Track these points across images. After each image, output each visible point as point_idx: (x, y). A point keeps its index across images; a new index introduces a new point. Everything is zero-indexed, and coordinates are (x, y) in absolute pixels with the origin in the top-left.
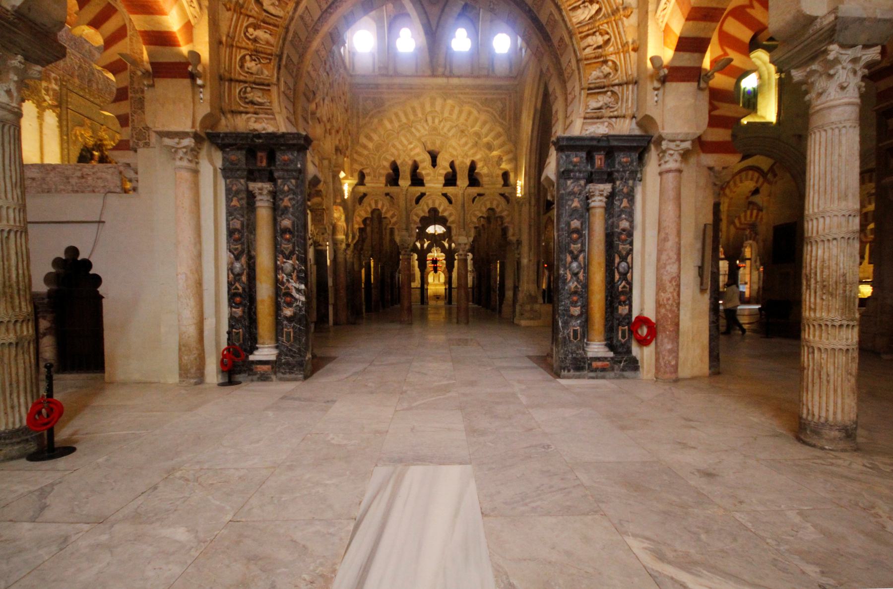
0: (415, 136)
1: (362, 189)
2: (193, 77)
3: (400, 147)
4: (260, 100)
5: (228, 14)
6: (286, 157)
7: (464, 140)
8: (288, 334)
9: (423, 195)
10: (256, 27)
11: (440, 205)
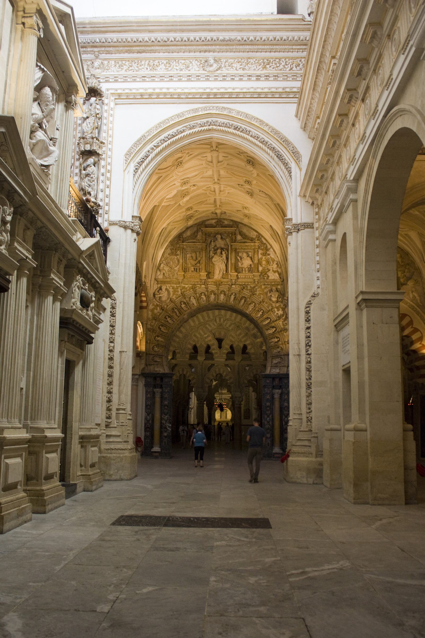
0: (209, 329)
1: (173, 362)
2: (140, 357)
3: (198, 336)
4: (158, 361)
5: (149, 332)
6: (166, 380)
7: (239, 332)
8: (165, 442)
9: (213, 365)
10: (158, 336)
11: (223, 373)
